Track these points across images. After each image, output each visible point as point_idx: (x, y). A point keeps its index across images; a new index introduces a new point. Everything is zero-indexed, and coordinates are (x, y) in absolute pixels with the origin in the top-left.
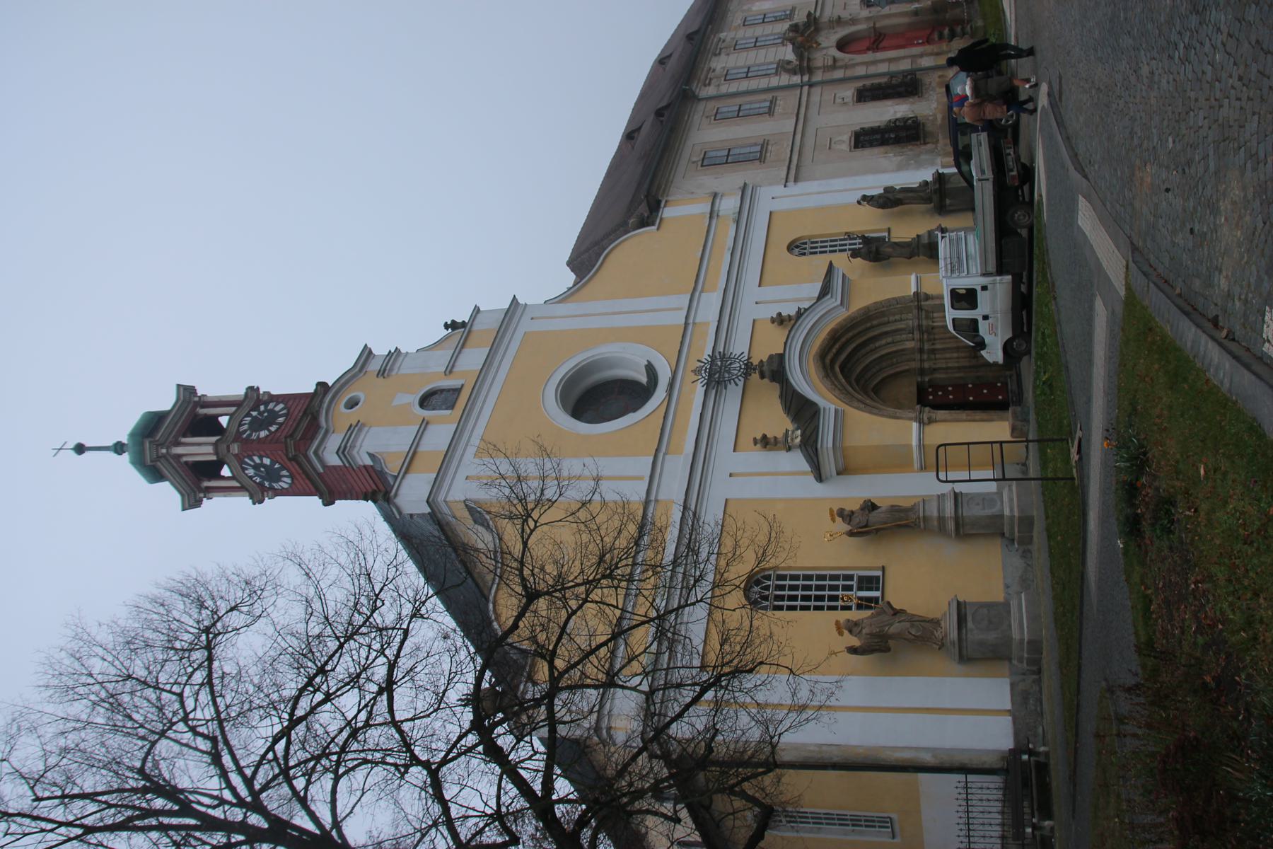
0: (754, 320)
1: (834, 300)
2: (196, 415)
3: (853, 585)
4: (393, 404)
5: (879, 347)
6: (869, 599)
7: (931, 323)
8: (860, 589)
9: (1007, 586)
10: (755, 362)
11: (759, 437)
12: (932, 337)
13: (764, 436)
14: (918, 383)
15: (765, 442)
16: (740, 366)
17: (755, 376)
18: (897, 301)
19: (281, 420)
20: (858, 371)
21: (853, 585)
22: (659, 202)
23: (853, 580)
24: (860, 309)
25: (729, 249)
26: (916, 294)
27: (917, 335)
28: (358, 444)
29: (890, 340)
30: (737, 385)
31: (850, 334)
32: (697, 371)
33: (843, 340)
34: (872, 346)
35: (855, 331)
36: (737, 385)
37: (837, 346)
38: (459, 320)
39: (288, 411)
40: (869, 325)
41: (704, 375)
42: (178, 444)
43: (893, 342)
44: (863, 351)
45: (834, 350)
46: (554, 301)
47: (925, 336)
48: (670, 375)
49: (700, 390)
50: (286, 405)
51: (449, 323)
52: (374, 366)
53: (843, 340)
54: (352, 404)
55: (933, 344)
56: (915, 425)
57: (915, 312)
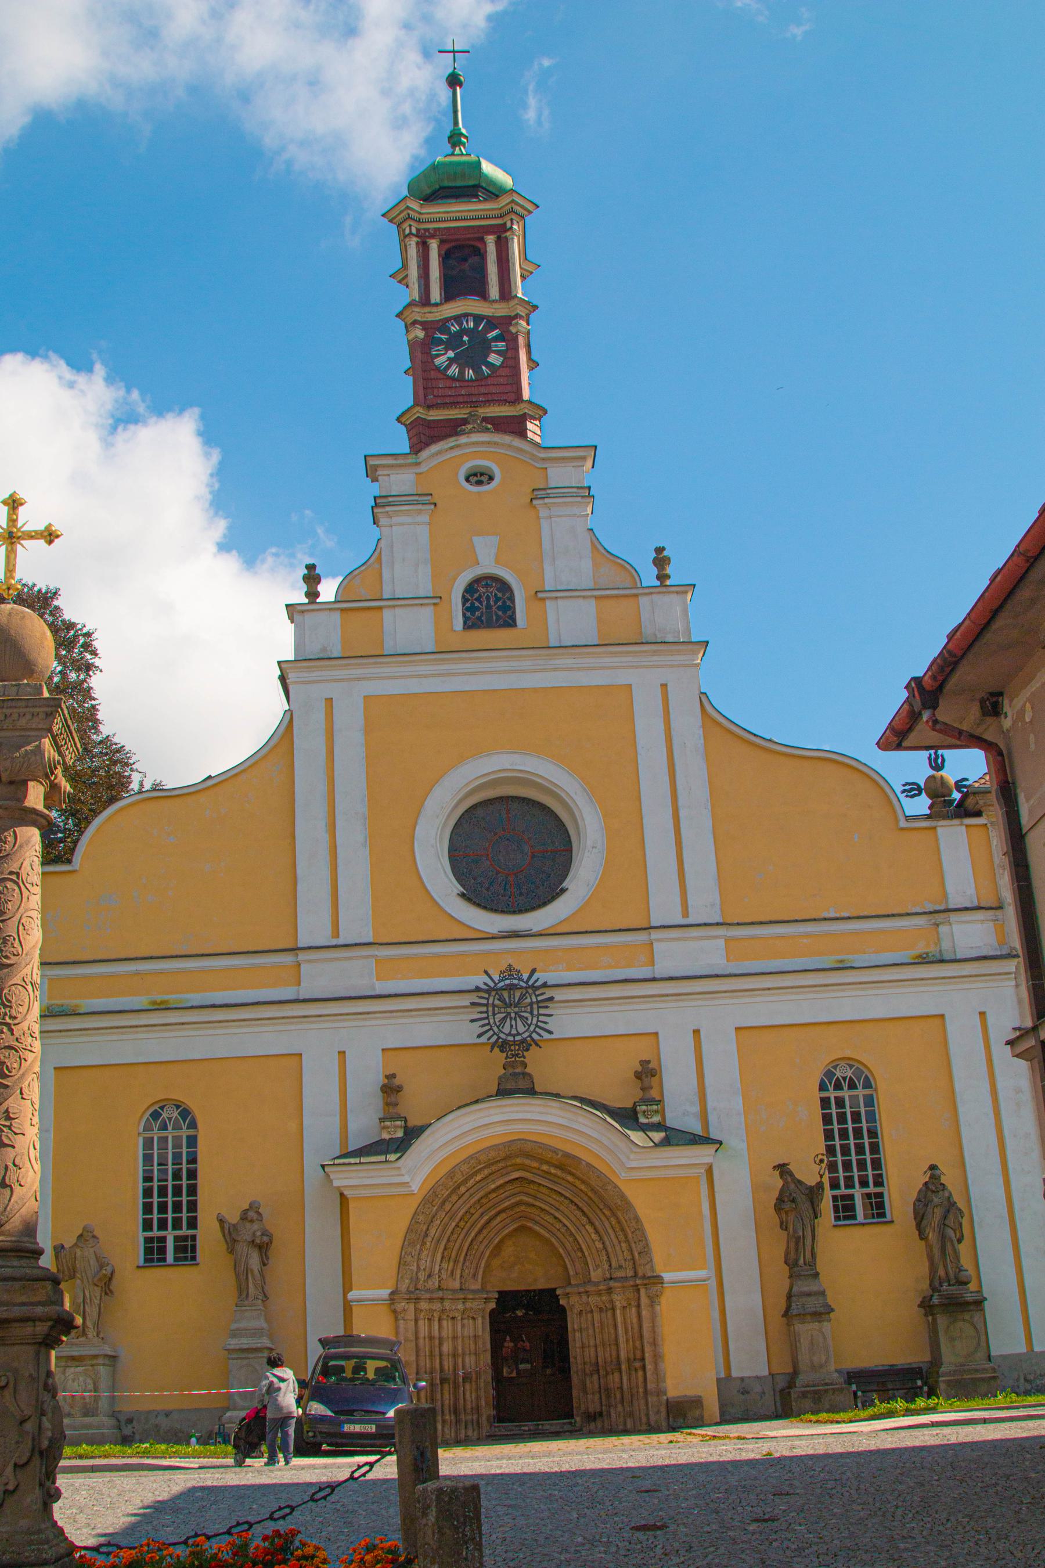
2: (482, 240)
3: (181, 1229)
4: (475, 539)
6: (163, 1250)
8: (177, 1239)
9: (167, 1414)
10: (532, 1056)
11: (397, 1082)
13: (399, 1089)
14: (555, 1290)
15: (391, 1089)
16: (518, 1034)
17: (499, 1057)
18: (646, 1251)
19: (470, 373)
21: (181, 1229)
22: (978, 814)
23: (188, 1229)
25: (841, 961)
26: (658, 1280)
28: (395, 520)
30: (480, 1036)
32: (510, 971)
36: (480, 1036)
38: (669, 570)
39: (489, 376)
41: (502, 984)
42: (423, 247)
46: (709, 708)
48: (536, 929)
49: (480, 980)
50: (502, 366)
51: (665, 553)
52: (559, 476)
54: (479, 477)
56: (385, 1293)
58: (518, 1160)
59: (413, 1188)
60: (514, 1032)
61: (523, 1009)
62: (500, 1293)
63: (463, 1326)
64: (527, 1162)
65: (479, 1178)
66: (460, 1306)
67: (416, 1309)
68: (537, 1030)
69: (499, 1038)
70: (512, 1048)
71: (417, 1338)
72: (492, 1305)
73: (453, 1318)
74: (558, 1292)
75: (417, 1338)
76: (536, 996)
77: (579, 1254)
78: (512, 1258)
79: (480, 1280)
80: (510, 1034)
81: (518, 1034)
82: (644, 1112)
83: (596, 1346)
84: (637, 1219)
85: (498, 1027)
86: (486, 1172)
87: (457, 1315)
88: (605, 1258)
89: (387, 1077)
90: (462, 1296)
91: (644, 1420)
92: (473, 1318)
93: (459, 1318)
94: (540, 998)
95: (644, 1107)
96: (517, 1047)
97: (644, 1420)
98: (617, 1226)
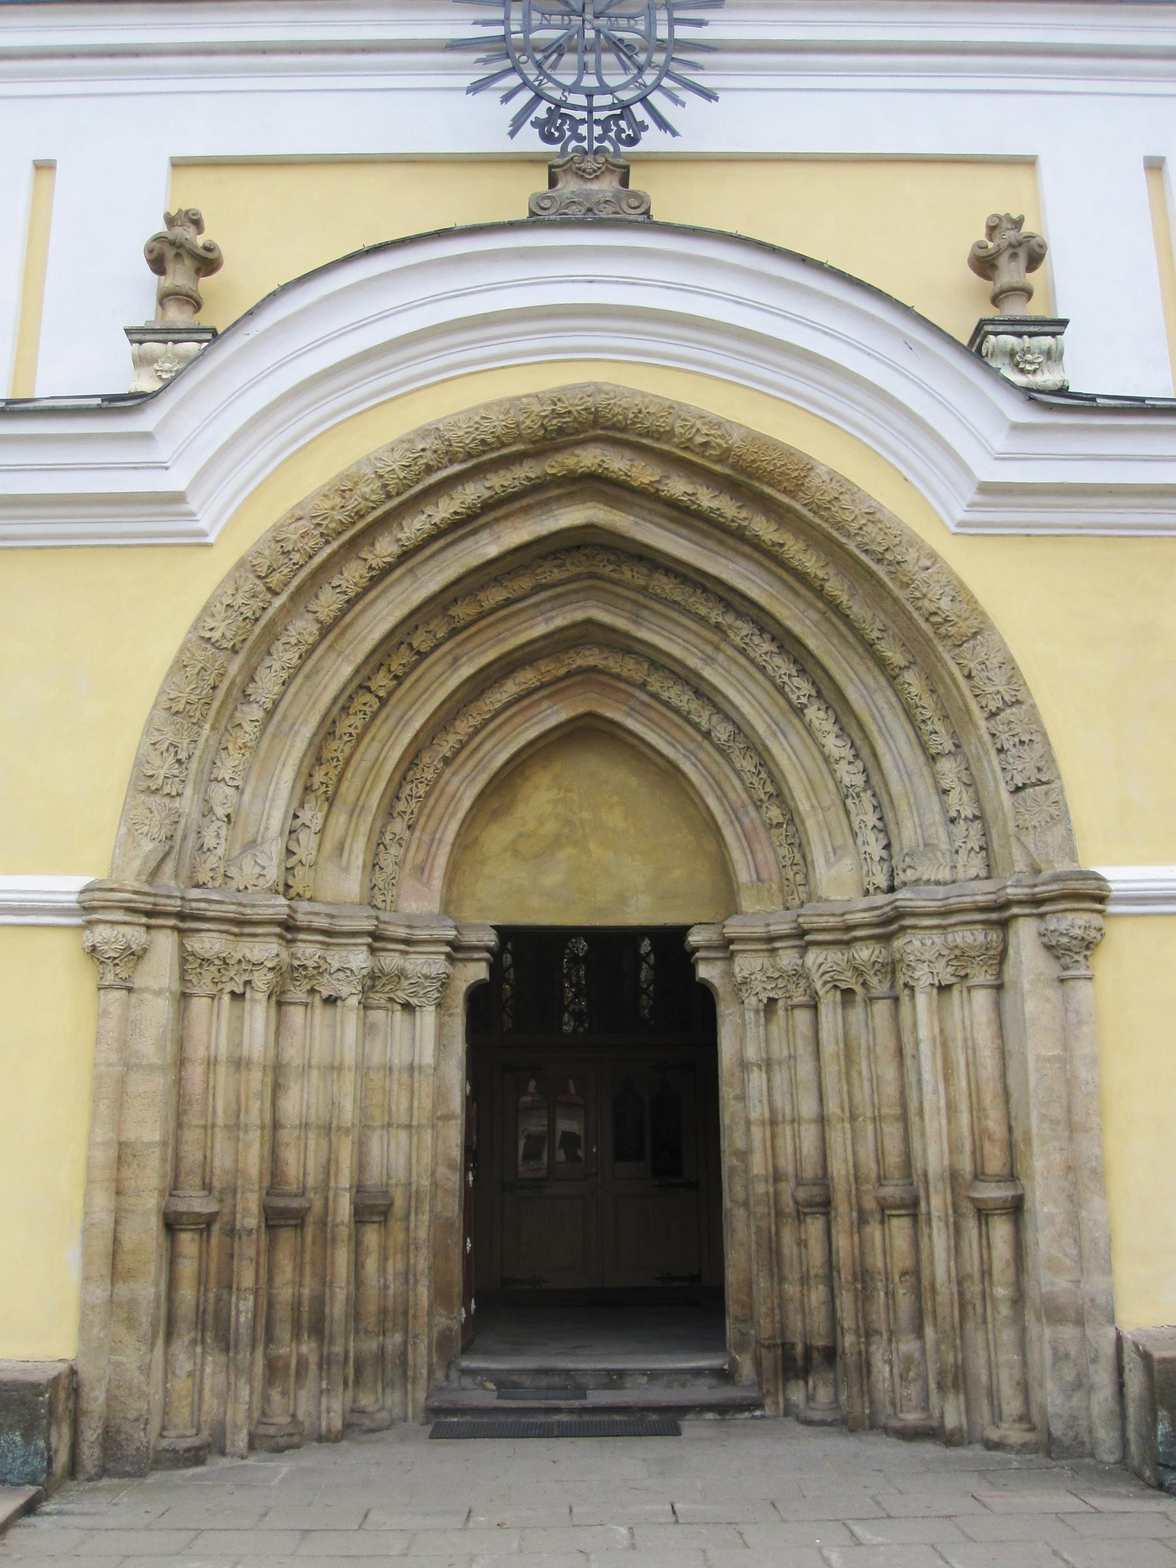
0: (1029, 162)
1: (1000, 442)
5: (808, 727)
7: (923, 977)
12: (879, 986)
14: (684, 930)
16: (604, 89)
20: (644, 634)
24: (960, 593)
27: (861, 910)
29: (850, 775)
31: (811, 563)
33: (764, 528)
34: (801, 688)
35: (836, 587)
37: (707, 499)
40: (895, 655)
43: (844, 795)
44: (763, 647)
45: (678, 487)
47: (864, 953)
53: (764, 528)
55: (848, 993)
57: (983, 893)
58: (589, 458)
59: (203, 524)
60: (590, 81)
61: (623, 23)
62: (503, 932)
63: (367, 1030)
64: (617, 463)
65: (443, 510)
66: (359, 959)
67: (184, 957)
68: (666, 82)
69: (539, 97)
70: (583, 130)
71: (181, 1062)
72: (478, 971)
73: (331, 1001)
74: (695, 938)
75: (181, 1062)
76: (673, 22)
77: (775, 813)
78: (550, 827)
79: (437, 882)
80: (575, 88)
81: (604, 89)
82: (1012, 354)
83: (822, 1120)
84: (1009, 665)
85: (539, 65)
86: (472, 493)
87: (345, 990)
88: (871, 819)
89: (170, 221)
90: (368, 925)
91: (1012, 1405)
92: (407, 1007)
93: (353, 1001)
94: (682, 32)
95: (1011, 340)
96: (598, 130)
97: (1012, 1405)
98: (927, 701)
